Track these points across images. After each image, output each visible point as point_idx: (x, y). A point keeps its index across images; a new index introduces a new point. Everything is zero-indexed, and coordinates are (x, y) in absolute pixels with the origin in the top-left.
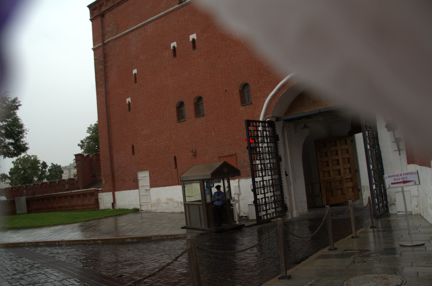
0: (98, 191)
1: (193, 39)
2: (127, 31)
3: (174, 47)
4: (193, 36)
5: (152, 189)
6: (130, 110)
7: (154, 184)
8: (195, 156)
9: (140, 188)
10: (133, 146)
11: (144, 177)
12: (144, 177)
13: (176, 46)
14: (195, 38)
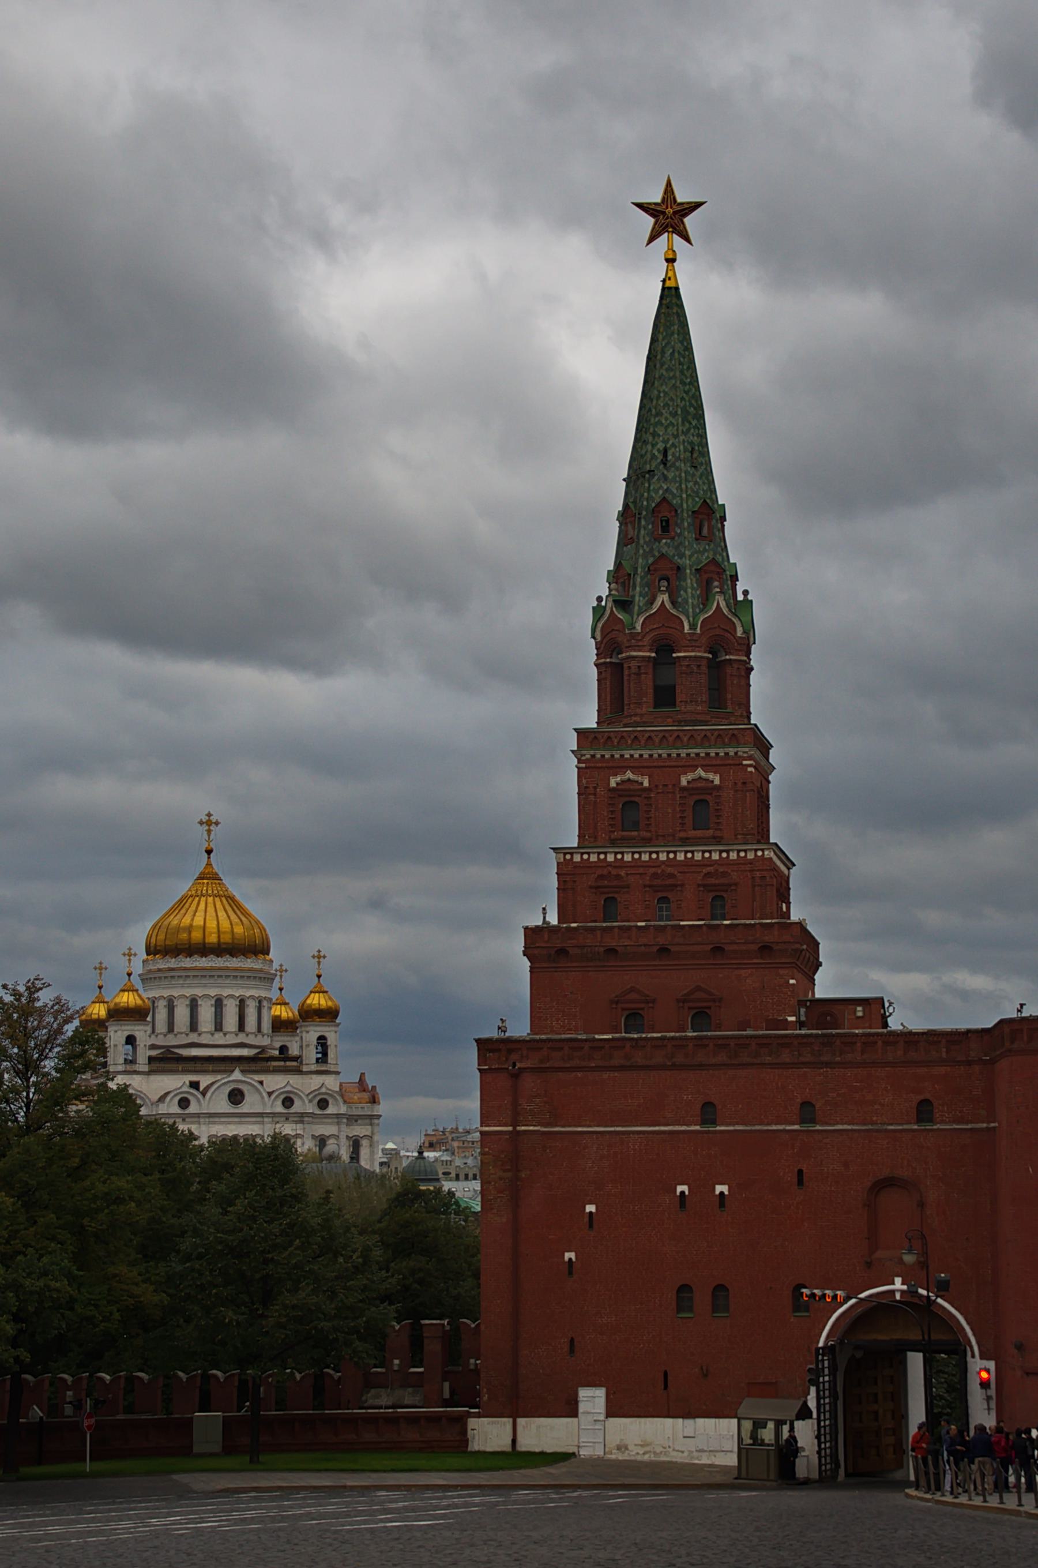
0: (469, 1415)
1: (722, 1193)
2: (580, 1129)
3: (682, 1193)
5: (611, 1420)
6: (570, 1273)
7: (612, 1412)
9: (580, 1415)
10: (572, 1340)
11: (593, 1399)
12: (593, 1399)
13: (687, 1193)
14: (726, 1193)
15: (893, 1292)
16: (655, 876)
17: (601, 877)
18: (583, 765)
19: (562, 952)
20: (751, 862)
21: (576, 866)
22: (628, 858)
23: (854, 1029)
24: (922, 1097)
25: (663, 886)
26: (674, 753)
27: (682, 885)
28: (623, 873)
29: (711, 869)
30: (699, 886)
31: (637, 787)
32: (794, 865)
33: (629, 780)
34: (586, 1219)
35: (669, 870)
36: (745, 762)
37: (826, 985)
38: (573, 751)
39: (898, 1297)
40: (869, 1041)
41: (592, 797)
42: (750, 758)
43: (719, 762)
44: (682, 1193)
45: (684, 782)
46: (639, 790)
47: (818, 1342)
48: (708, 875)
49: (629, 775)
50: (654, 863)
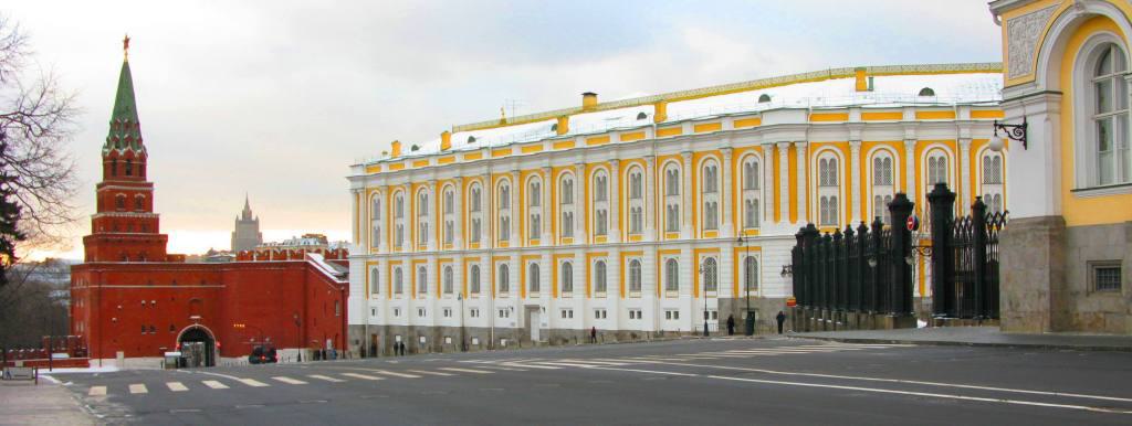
7: (126, 356)
11: (120, 354)
12: (120, 354)
23: (179, 264)
25: (132, 223)
37: (171, 249)
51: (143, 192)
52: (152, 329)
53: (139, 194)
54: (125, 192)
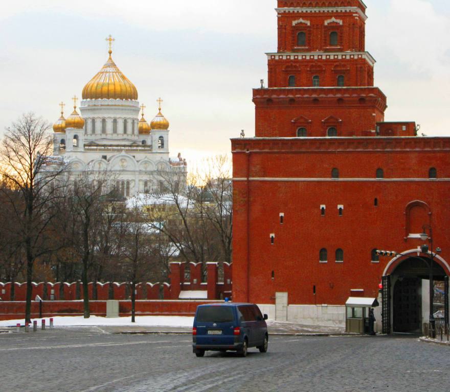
1: (340, 209)
3: (323, 208)
4: (340, 206)
5: (290, 305)
7: (291, 301)
8: (332, 288)
10: (273, 272)
11: (282, 297)
12: (282, 297)
13: (325, 208)
14: (343, 208)
15: (416, 253)
16: (312, 66)
17: (287, 67)
18: (280, 16)
19: (270, 100)
20: (356, 60)
21: (276, 61)
22: (300, 58)
24: (431, 167)
25: (316, 69)
26: (322, 10)
27: (324, 71)
28: (298, 65)
29: (337, 63)
30: (332, 71)
31: (304, 25)
32: (376, 62)
33: (301, 23)
34: (280, 219)
35: (319, 64)
36: (354, 15)
37: (390, 116)
38: (276, 9)
39: (418, 254)
40: (407, 142)
41: (284, 31)
42: (356, 13)
43: (342, 15)
44: (323, 208)
45: (326, 23)
46: (305, 27)
47: (382, 274)
48: (337, 66)
49: (301, 20)
50: (312, 60)
51: (337, 15)
52: (339, 253)
53: (333, 19)
54: (305, 16)
